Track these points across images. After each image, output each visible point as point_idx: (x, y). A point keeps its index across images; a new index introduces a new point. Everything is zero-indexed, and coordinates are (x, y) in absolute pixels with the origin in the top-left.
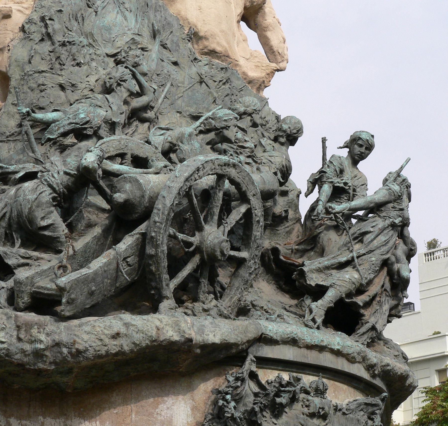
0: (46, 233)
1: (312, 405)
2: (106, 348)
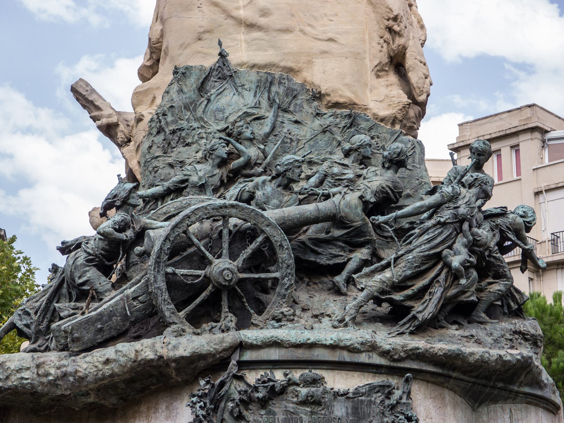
0: (85, 288)
1: (300, 395)
2: (101, 372)
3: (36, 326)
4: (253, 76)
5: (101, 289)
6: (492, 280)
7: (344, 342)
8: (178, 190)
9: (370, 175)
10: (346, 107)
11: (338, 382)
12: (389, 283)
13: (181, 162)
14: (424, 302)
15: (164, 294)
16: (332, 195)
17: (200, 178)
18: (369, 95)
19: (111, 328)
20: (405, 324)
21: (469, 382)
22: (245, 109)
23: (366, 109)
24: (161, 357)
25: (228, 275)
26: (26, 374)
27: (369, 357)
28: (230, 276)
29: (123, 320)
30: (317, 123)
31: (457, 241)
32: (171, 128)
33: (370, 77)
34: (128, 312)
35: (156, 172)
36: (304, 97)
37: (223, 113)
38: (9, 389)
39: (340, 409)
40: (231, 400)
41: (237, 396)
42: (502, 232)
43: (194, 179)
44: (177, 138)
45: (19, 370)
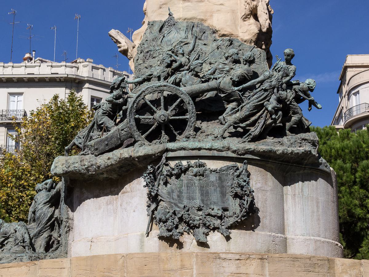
0: (103, 126)
2: (107, 164)
3: (84, 143)
4: (185, 24)
5: (109, 126)
7: (214, 147)
8: (148, 79)
9: (236, 68)
10: (228, 36)
11: (211, 165)
12: (239, 119)
13: (151, 66)
14: (256, 127)
15: (134, 127)
16: (218, 78)
17: (158, 73)
18: (239, 29)
19: (112, 144)
20: (246, 137)
21: (278, 163)
22: (180, 40)
23: (238, 37)
24: (131, 156)
25: (163, 118)
26: (76, 165)
27: (227, 153)
28: (164, 118)
29: (117, 140)
30: (215, 45)
31: (272, 97)
32: (146, 50)
33: (240, 21)
34: (119, 136)
35: (140, 71)
36: (208, 32)
37: (171, 42)
38: (70, 172)
39: (213, 178)
40: (162, 175)
41: (165, 173)
42: (296, 92)
43: (155, 74)
44: (149, 55)
45: (73, 163)
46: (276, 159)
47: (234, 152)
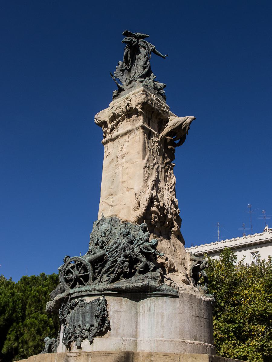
6: (140, 263)
11: (89, 300)
18: (131, 216)
39: (88, 307)
46: (125, 292)
47: (98, 291)
